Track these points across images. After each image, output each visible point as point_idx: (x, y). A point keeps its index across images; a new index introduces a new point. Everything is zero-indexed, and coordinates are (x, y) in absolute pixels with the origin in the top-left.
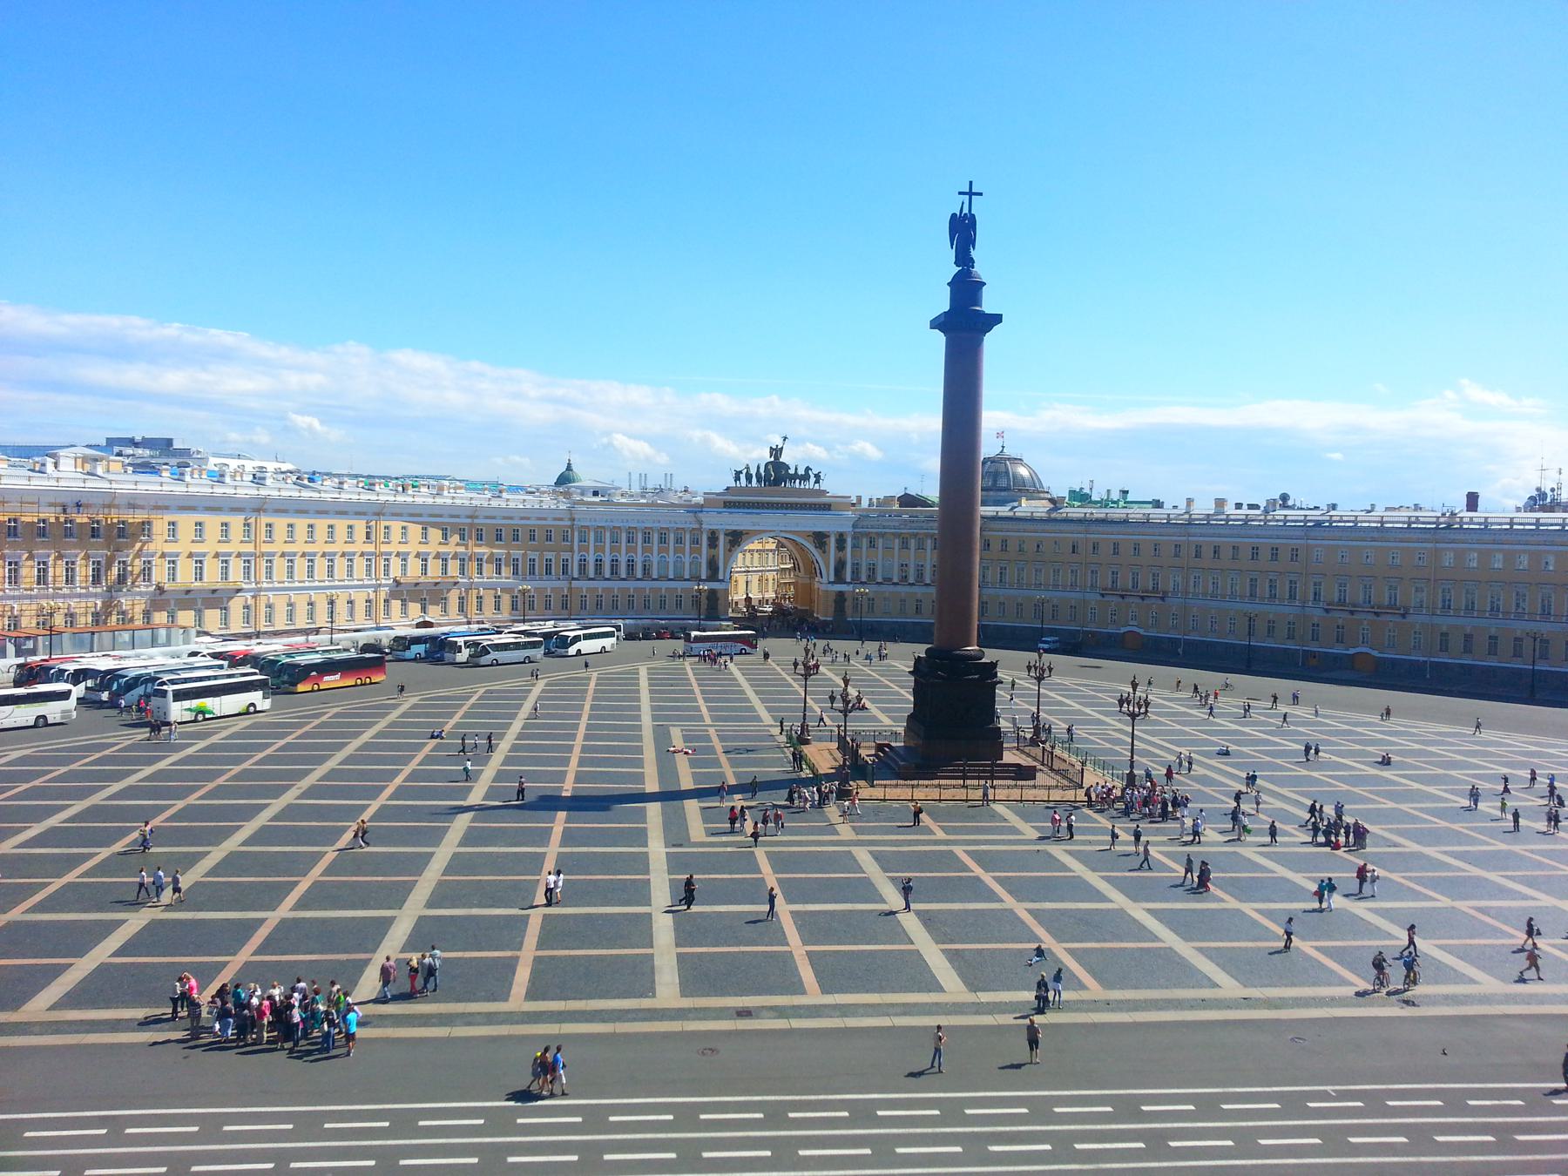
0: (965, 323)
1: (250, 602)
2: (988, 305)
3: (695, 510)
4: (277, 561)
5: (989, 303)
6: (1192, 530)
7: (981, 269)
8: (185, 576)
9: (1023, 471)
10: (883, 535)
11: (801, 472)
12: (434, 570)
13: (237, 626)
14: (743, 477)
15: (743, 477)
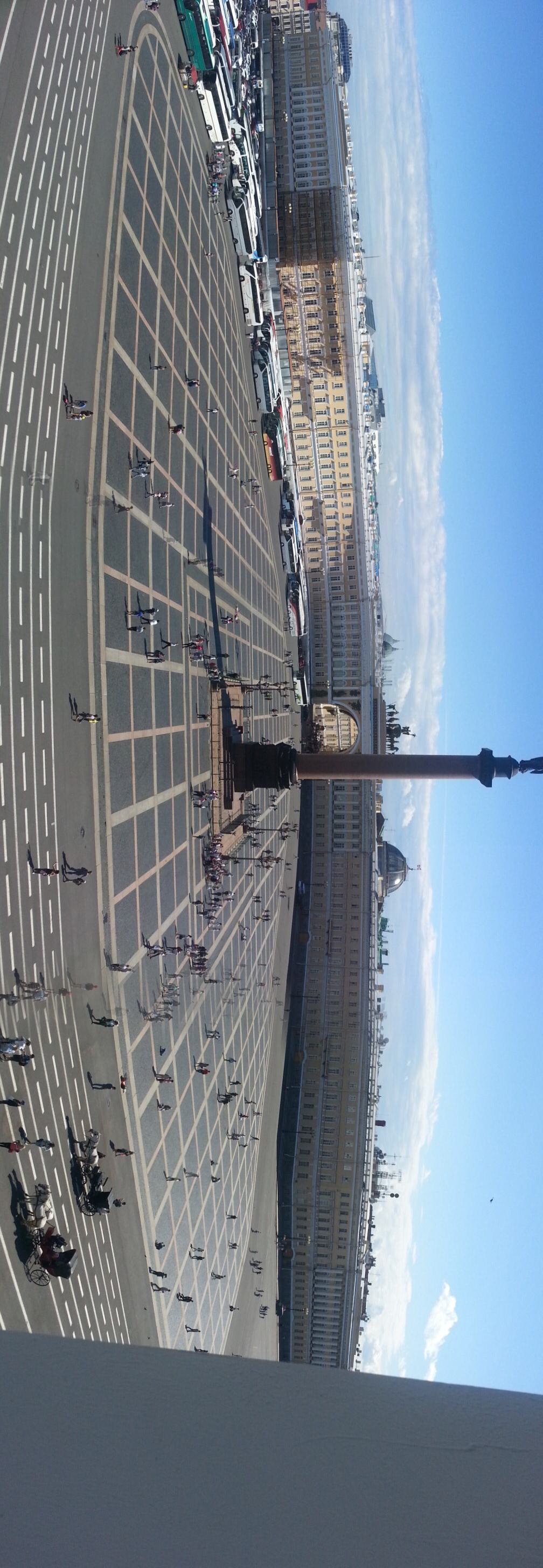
0: (485, 767)
1: (307, 427)
2: (496, 780)
3: (372, 681)
4: (328, 438)
5: (498, 781)
6: (366, 971)
7: (518, 776)
8: (317, 394)
9: (397, 881)
10: (360, 795)
11: (395, 745)
12: (330, 523)
13: (295, 421)
14: (391, 710)
15: (391, 710)
